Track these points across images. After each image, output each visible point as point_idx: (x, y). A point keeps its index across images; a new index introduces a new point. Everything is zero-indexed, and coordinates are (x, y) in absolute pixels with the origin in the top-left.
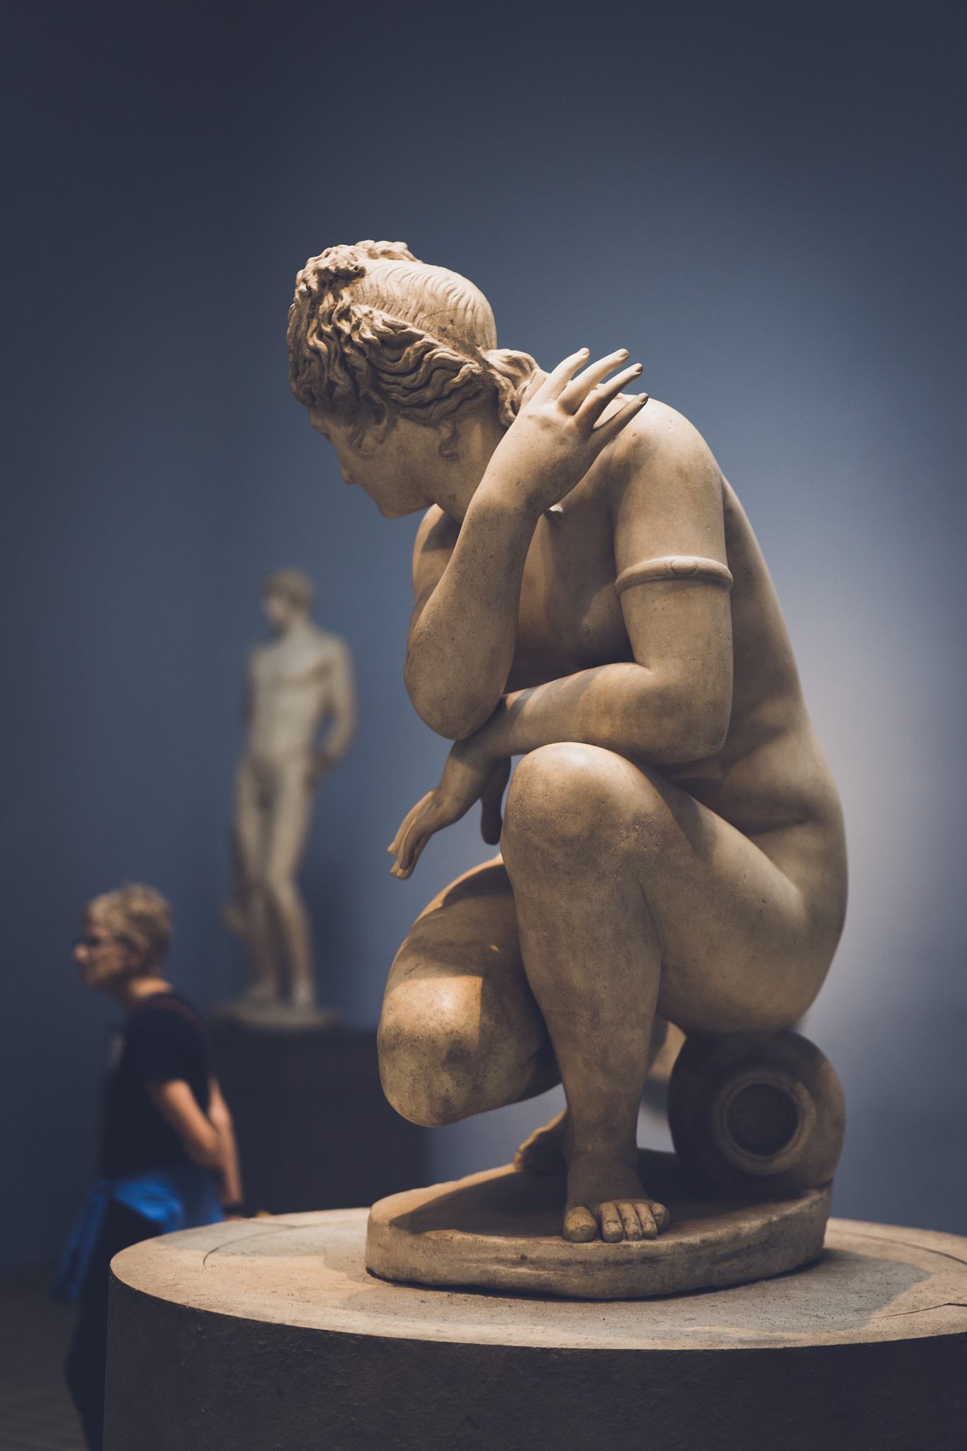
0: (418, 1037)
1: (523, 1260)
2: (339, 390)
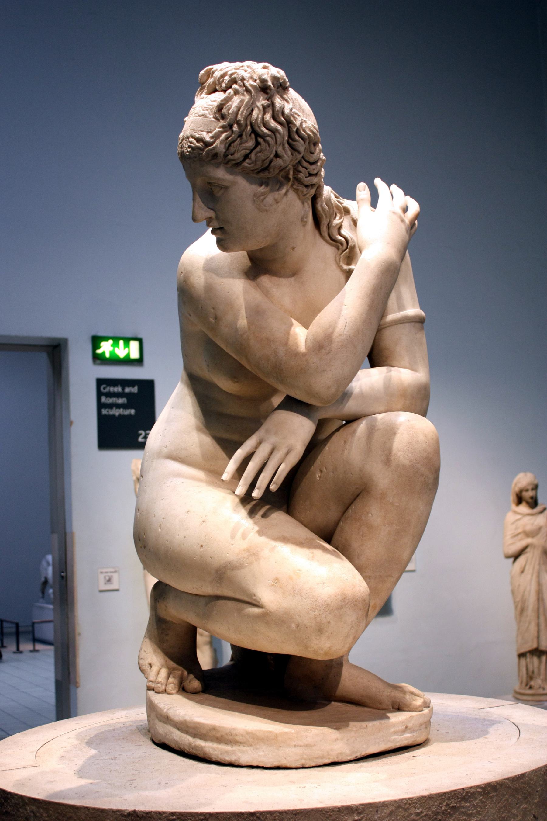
0: (357, 599)
1: (407, 729)
2: (279, 162)
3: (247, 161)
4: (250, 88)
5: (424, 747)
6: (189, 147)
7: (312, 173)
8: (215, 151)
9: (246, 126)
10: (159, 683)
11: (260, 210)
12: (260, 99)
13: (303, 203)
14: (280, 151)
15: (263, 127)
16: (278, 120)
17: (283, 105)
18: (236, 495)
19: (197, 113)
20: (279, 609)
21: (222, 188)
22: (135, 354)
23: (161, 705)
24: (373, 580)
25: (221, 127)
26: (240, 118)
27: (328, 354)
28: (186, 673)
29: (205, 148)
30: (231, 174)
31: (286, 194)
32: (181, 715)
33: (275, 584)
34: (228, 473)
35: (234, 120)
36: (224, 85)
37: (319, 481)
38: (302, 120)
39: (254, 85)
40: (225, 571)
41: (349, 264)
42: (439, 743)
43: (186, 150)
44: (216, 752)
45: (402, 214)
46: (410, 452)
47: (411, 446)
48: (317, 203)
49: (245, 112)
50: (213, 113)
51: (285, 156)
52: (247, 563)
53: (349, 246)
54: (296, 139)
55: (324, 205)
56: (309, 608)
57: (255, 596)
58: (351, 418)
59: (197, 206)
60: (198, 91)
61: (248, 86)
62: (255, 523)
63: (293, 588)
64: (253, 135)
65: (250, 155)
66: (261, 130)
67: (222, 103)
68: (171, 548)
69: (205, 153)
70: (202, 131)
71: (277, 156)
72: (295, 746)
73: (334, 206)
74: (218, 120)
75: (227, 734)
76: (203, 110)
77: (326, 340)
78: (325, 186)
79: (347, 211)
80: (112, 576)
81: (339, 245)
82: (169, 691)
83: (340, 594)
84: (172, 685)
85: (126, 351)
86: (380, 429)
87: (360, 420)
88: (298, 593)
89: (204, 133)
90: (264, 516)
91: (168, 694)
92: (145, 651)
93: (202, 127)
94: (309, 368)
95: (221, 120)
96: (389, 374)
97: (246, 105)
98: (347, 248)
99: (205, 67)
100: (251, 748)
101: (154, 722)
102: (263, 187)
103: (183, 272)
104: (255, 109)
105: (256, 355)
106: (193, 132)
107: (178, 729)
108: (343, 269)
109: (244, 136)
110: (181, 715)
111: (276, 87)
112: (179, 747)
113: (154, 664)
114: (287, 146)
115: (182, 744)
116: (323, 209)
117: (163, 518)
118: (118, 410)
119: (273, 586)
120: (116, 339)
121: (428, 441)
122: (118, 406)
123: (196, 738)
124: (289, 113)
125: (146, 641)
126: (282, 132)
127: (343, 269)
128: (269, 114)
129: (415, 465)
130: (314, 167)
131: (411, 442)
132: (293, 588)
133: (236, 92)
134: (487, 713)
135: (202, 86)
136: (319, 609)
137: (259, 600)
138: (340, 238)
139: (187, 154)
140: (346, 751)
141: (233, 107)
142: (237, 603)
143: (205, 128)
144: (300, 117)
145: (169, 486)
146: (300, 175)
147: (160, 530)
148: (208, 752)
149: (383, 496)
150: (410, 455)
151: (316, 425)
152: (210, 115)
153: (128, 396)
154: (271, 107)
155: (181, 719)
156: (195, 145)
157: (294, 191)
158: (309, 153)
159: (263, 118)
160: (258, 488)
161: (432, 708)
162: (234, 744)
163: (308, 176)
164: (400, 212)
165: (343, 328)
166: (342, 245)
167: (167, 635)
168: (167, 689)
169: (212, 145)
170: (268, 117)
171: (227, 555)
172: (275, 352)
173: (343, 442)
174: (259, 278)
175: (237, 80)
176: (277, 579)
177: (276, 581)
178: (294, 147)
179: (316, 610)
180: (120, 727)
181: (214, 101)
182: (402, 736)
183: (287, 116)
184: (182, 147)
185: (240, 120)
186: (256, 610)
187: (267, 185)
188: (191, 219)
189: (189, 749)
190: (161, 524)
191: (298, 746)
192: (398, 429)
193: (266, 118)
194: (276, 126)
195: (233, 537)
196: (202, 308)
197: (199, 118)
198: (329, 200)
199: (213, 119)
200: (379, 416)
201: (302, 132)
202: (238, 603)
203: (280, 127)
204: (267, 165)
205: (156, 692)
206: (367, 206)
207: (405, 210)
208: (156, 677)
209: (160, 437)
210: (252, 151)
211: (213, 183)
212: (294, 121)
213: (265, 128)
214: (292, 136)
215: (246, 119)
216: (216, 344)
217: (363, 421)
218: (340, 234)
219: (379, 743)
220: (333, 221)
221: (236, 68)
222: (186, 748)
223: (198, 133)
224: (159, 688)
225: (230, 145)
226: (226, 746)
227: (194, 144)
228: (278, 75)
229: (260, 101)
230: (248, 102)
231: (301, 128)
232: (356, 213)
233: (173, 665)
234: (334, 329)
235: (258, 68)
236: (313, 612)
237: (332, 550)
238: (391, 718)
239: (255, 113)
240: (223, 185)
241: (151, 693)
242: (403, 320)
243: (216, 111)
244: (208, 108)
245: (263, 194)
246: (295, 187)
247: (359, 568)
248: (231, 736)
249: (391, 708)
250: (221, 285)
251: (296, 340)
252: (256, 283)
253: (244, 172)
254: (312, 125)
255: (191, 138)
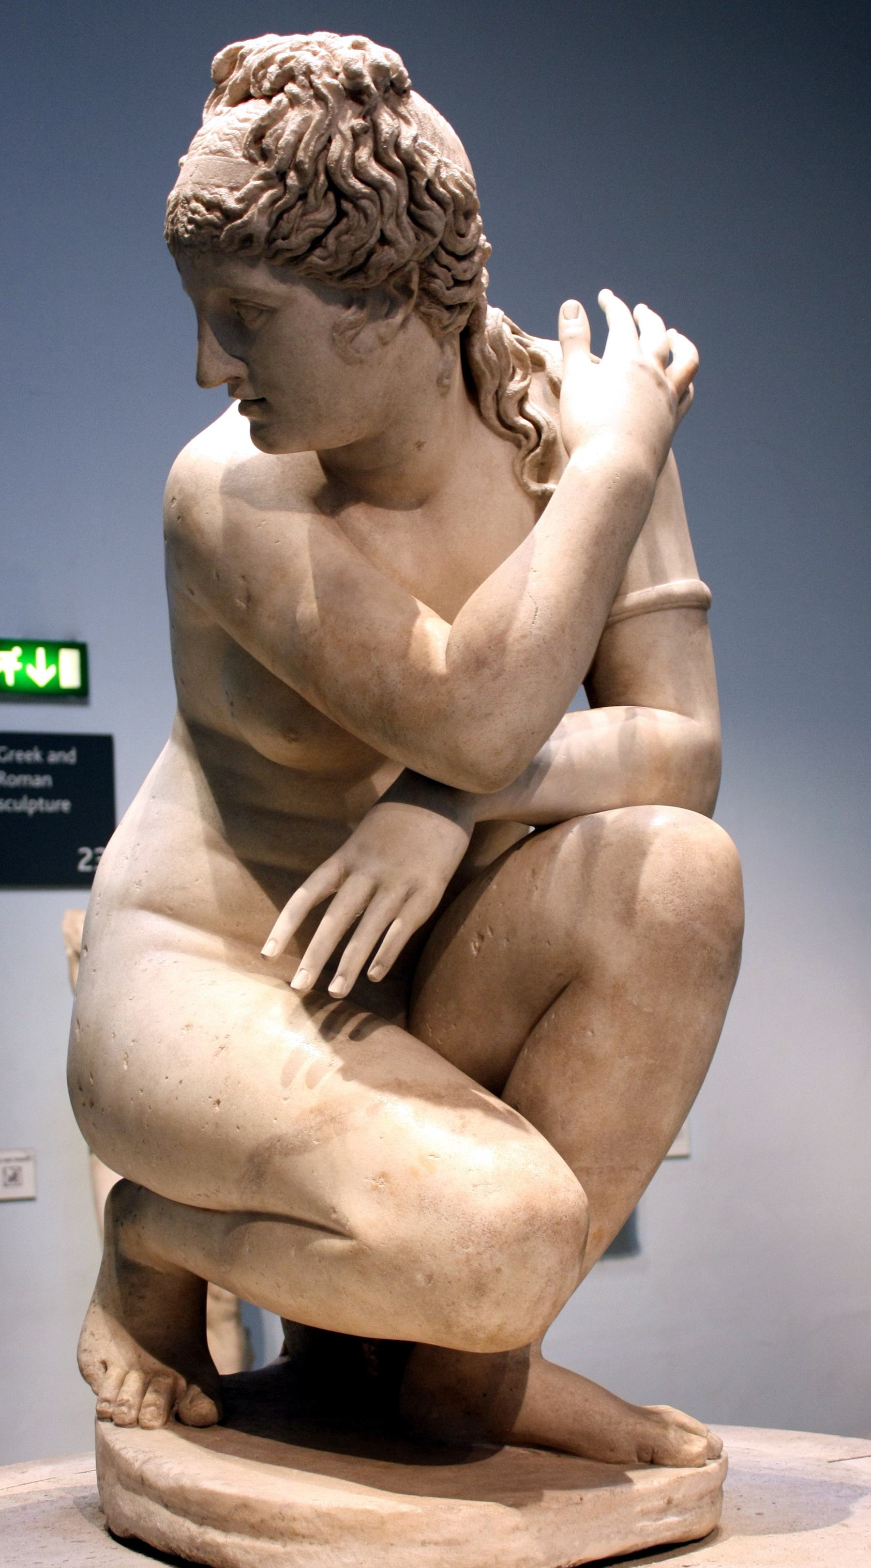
0: (561, 1219)
2: (388, 254)
3: (318, 252)
4: (324, 91)
5: (709, 1546)
6: (191, 221)
7: (461, 277)
8: (249, 230)
9: (316, 174)
10: (123, 1405)
11: (347, 360)
12: (346, 115)
13: (441, 345)
14: (391, 229)
15: (354, 178)
16: (386, 161)
17: (397, 128)
18: (294, 990)
19: (207, 147)
20: (389, 1240)
21: (262, 311)
22: (70, 679)
23: (128, 1453)
24: (595, 1178)
25: (261, 177)
26: (302, 158)
27: (497, 677)
28: (182, 1382)
29: (226, 224)
30: (283, 280)
31: (404, 324)
32: (171, 1475)
33: (380, 1186)
34: (276, 941)
35: (290, 162)
36: (266, 85)
37: (476, 958)
38: (439, 161)
39: (334, 85)
40: (269, 1157)
41: (542, 479)
42: (741, 1537)
43: (184, 229)
44: (249, 1558)
45: (660, 370)
46: (677, 895)
47: (679, 881)
48: (473, 346)
49: (313, 143)
50: (243, 145)
51: (402, 240)
52: (318, 1140)
53: (542, 441)
54: (425, 203)
55: (489, 351)
56: (454, 1240)
57: (335, 1212)
58: (548, 820)
59: (207, 351)
60: (209, 98)
61: (320, 86)
62: (337, 1052)
63: (420, 1195)
64: (331, 196)
65: (324, 240)
66: (349, 185)
67: (263, 124)
68: (150, 1107)
69: (225, 235)
70: (218, 186)
71: (384, 240)
72: (424, 1543)
73: (509, 351)
74: (253, 161)
75: (273, 1518)
76: (221, 140)
77: (492, 648)
78: (489, 307)
79: (538, 363)
80: (20, 1169)
81: (521, 437)
82: (146, 1421)
83: (522, 1207)
84: (153, 1408)
85: (52, 671)
86: (612, 845)
87: (566, 824)
88: (430, 1205)
89: (224, 191)
90: (356, 1035)
91: (144, 1428)
92: (92, 1334)
93: (218, 178)
94: (453, 709)
95: (261, 163)
96: (631, 721)
97: (316, 128)
98: (537, 445)
99: (225, 46)
100: (328, 1548)
101: (113, 1490)
102: (353, 309)
103: (177, 497)
104: (335, 138)
105: (337, 681)
106: (199, 189)
107: (166, 1506)
108: (530, 490)
109: (311, 198)
110: (171, 1475)
111: (383, 89)
112: (167, 1545)
113: (113, 1363)
114: (405, 219)
115: (174, 1538)
116: (486, 359)
117: (133, 1041)
118: (32, 802)
119: (374, 1190)
120: (29, 645)
121: (717, 871)
122: (34, 793)
123: (206, 1527)
124: (410, 145)
125: (94, 1312)
126: (395, 189)
127: (530, 490)
128: (367, 148)
129: (689, 924)
130: (465, 264)
131: (679, 872)
132: (420, 1195)
133: (294, 101)
134: (848, 1470)
135: (219, 87)
136: (477, 1242)
137: (343, 1221)
138: (523, 421)
139: (186, 236)
140: (537, 1553)
141: (287, 132)
142: (296, 1227)
143: (226, 179)
144: (435, 155)
145: (146, 969)
146: (434, 283)
147: (125, 1067)
148: (232, 1557)
149: (618, 990)
150: (677, 901)
151: (471, 836)
152: (236, 150)
153: (56, 770)
154: (370, 133)
155: (172, 1484)
156: (204, 217)
157: (421, 318)
158: (455, 234)
159: (353, 158)
160: (341, 975)
161: (726, 1460)
162: (289, 1538)
163: (453, 286)
164: (655, 364)
165: (530, 621)
166: (527, 436)
167: (142, 1298)
168: (141, 1417)
169: (241, 217)
170: (364, 154)
171: (275, 1121)
172: (379, 673)
173: (529, 873)
174: (343, 510)
175: (296, 73)
176: (383, 1175)
177: (382, 1179)
178: (421, 221)
179: (470, 1243)
180: (37, 1501)
181: (246, 120)
182: (660, 1522)
183: (407, 152)
184: (175, 221)
185: (301, 162)
186: (337, 1244)
187: (362, 305)
188: (195, 381)
189: (190, 1550)
190: (128, 1053)
191: (429, 1543)
192: (651, 844)
193: (360, 158)
194: (382, 176)
195: (286, 1081)
196: (218, 576)
197: (211, 156)
198: (498, 338)
199: (243, 160)
200: (610, 816)
201: (438, 188)
202: (297, 1227)
203: (391, 178)
204: (361, 260)
205: (117, 1425)
206: (582, 352)
207: (667, 360)
208: (117, 1391)
209: (126, 861)
210: (328, 229)
211: (243, 300)
212: (422, 164)
213: (356, 180)
214: (418, 196)
215: (315, 160)
216: (249, 656)
217: (574, 826)
218: (523, 414)
219: (608, 1537)
220: (508, 385)
221: (294, 47)
222: (183, 1548)
223: (209, 191)
224: (123, 1416)
225: (280, 217)
226: (273, 1543)
227: (201, 214)
228: (386, 63)
229: (347, 121)
230: (320, 121)
231: (437, 180)
232: (558, 367)
233: (154, 1364)
234: (510, 623)
235: (341, 48)
236: (463, 1248)
237: (504, 1112)
238: (635, 1481)
239: (336, 146)
240: (265, 306)
241: (106, 1427)
242: (663, 604)
243: (250, 142)
244: (231, 136)
245: (353, 325)
246: (423, 309)
247: (566, 1152)
248: (283, 1520)
249: (636, 1459)
250: (259, 526)
251: (425, 647)
252: (338, 523)
253: (312, 276)
254: (462, 173)
255: (194, 201)
